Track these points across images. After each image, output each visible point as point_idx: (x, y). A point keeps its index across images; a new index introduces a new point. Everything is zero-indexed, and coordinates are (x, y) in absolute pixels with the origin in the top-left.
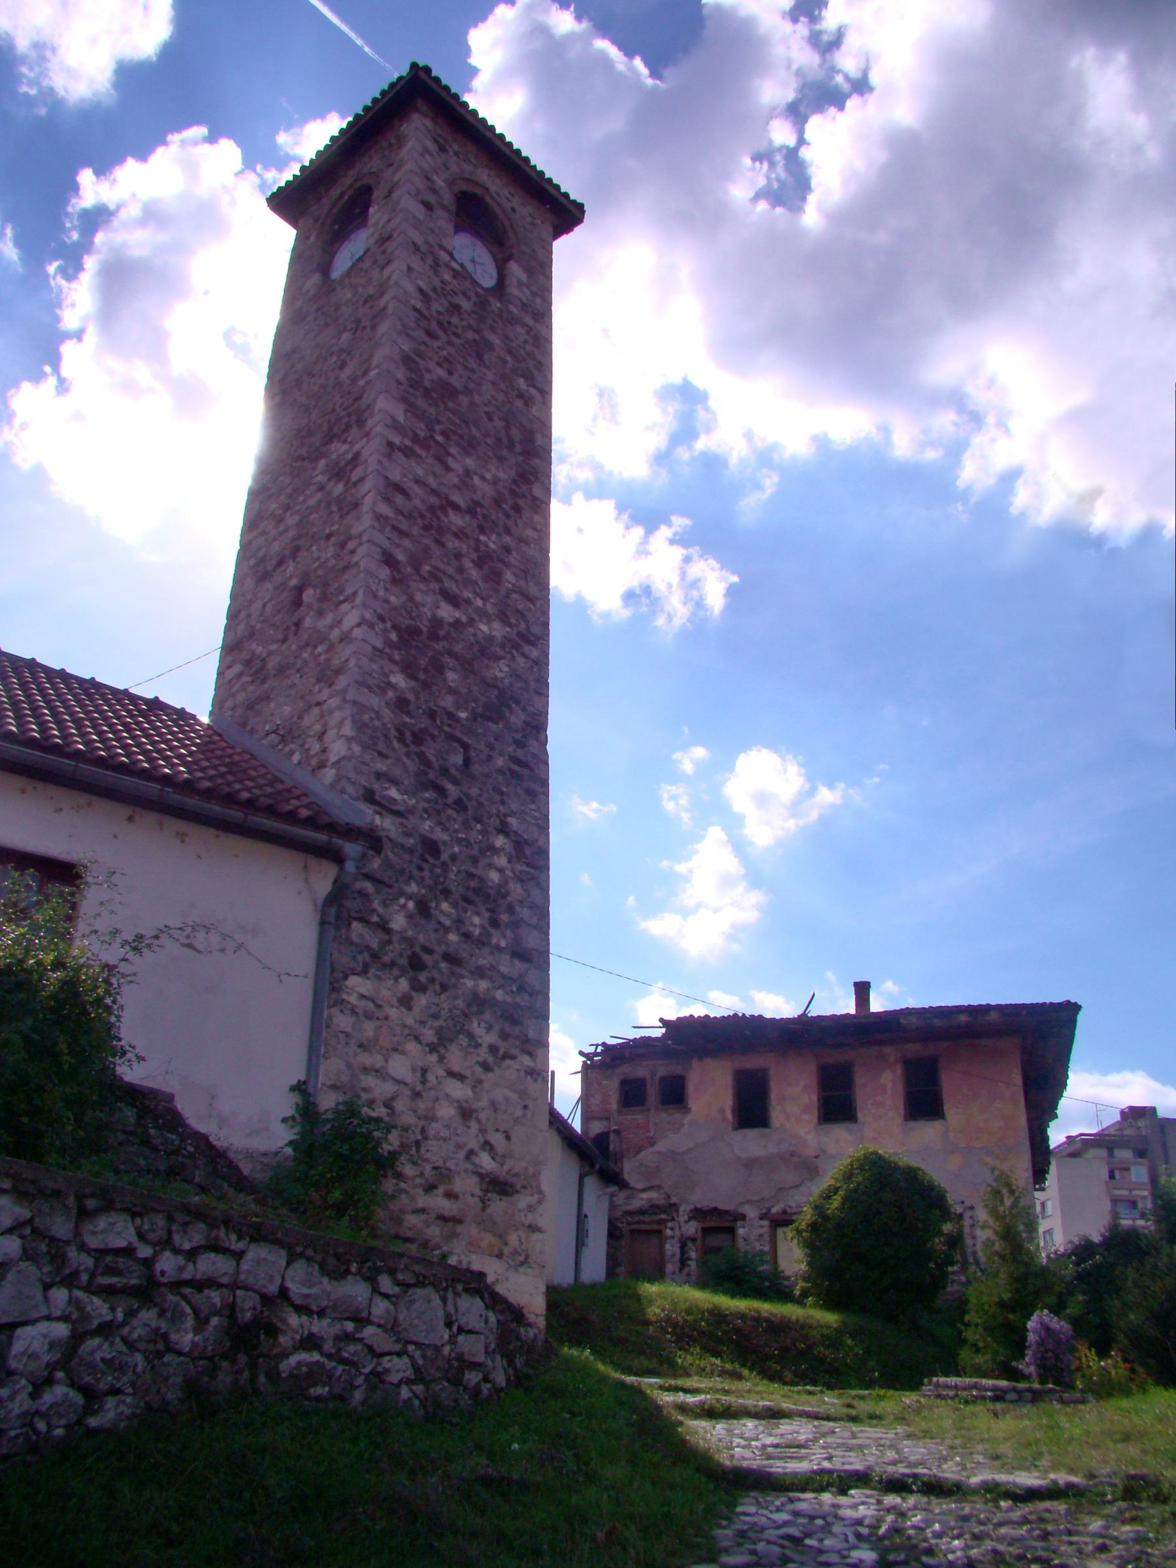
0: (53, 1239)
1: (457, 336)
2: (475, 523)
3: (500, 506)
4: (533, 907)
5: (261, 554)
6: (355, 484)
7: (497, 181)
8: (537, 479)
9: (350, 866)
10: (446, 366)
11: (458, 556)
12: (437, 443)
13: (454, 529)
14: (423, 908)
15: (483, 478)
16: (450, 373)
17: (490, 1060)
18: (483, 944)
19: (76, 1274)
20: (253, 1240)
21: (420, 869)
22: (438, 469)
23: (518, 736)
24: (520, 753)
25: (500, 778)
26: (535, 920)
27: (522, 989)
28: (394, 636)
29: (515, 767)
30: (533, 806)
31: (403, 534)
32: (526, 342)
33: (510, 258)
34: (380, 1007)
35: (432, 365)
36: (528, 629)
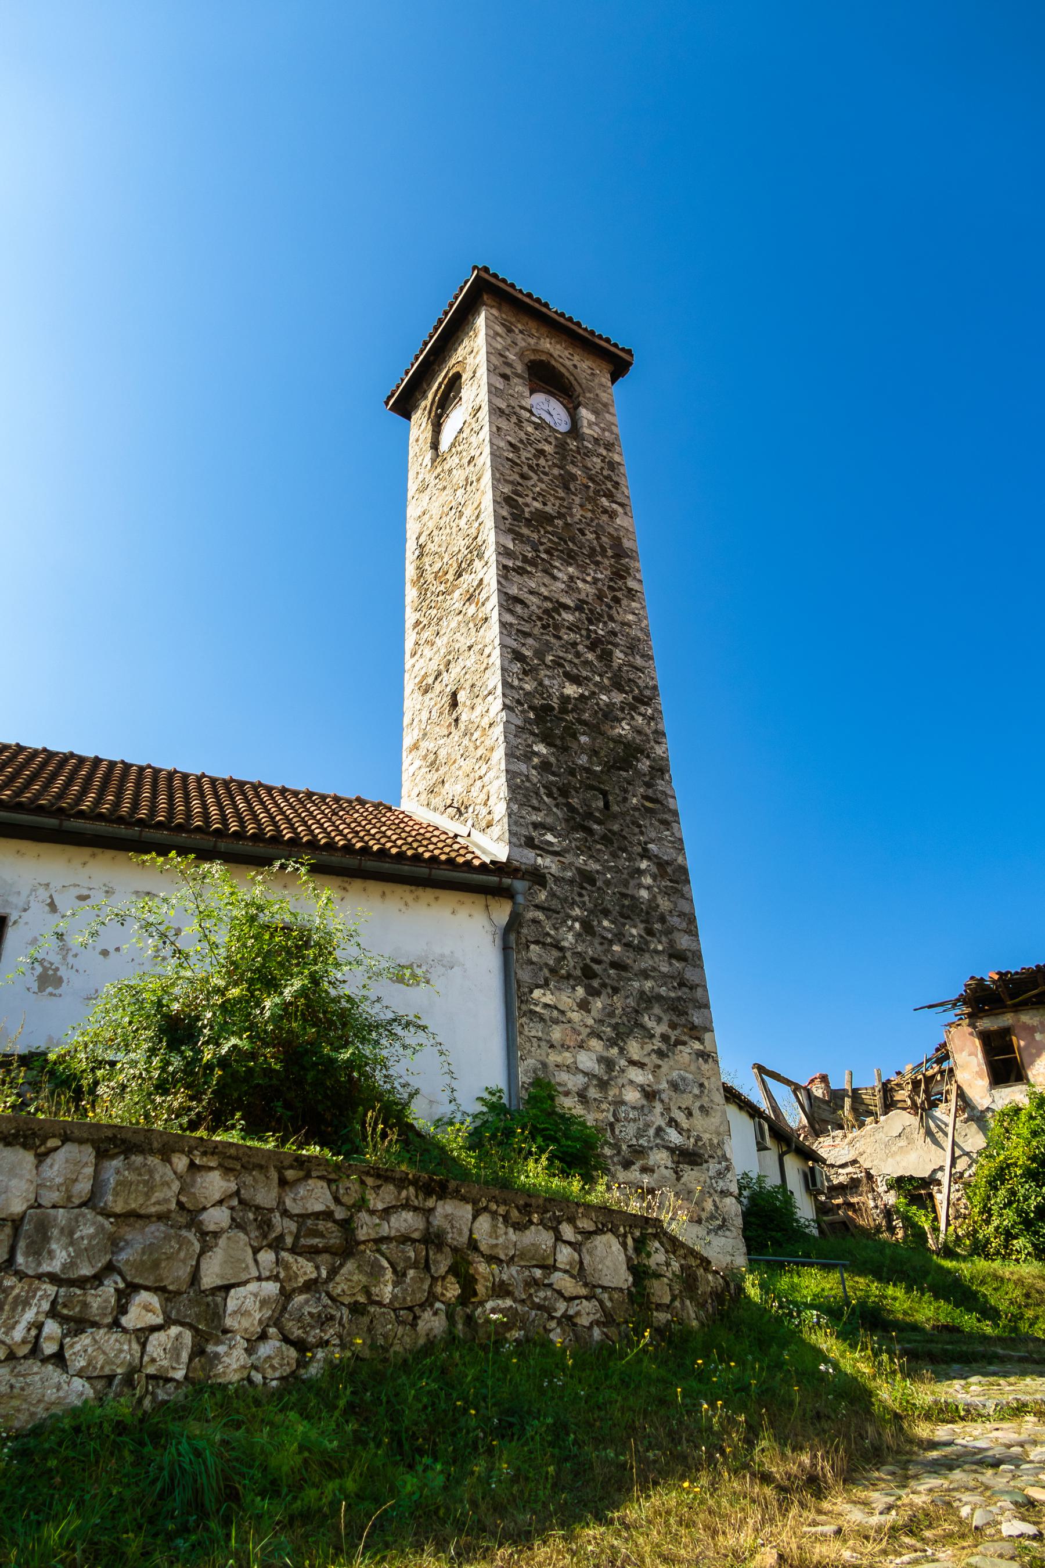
0: (258, 1208)
1: (545, 474)
4: (682, 915)
5: (422, 673)
7: (558, 346)
9: (520, 899)
10: (540, 499)
11: (574, 644)
12: (543, 559)
14: (588, 928)
15: (584, 581)
16: (545, 504)
17: (664, 1047)
18: (643, 950)
19: (281, 1237)
20: (440, 1198)
21: (581, 895)
22: (547, 580)
23: (647, 779)
24: (650, 792)
25: (637, 814)
26: (684, 925)
27: (682, 984)
28: (532, 715)
29: (648, 804)
30: (667, 833)
31: (527, 635)
32: (602, 468)
33: (579, 404)
34: (563, 1012)
35: (529, 500)
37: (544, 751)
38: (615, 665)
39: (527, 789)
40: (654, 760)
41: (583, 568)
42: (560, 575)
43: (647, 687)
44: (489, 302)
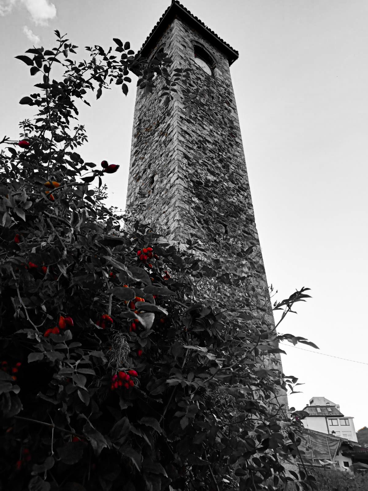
1: (201, 87)
2: (217, 148)
3: (225, 144)
6: (169, 134)
7: (207, 44)
8: (237, 137)
11: (212, 158)
12: (199, 120)
13: (209, 149)
15: (217, 133)
22: (200, 128)
23: (245, 223)
24: (246, 229)
28: (192, 184)
29: (245, 234)
32: (225, 93)
33: (215, 67)
36: (242, 186)
37: (198, 201)
38: (230, 172)
39: (189, 217)
40: (248, 215)
41: (217, 128)
42: (206, 128)
43: (244, 184)
44: (178, 18)
